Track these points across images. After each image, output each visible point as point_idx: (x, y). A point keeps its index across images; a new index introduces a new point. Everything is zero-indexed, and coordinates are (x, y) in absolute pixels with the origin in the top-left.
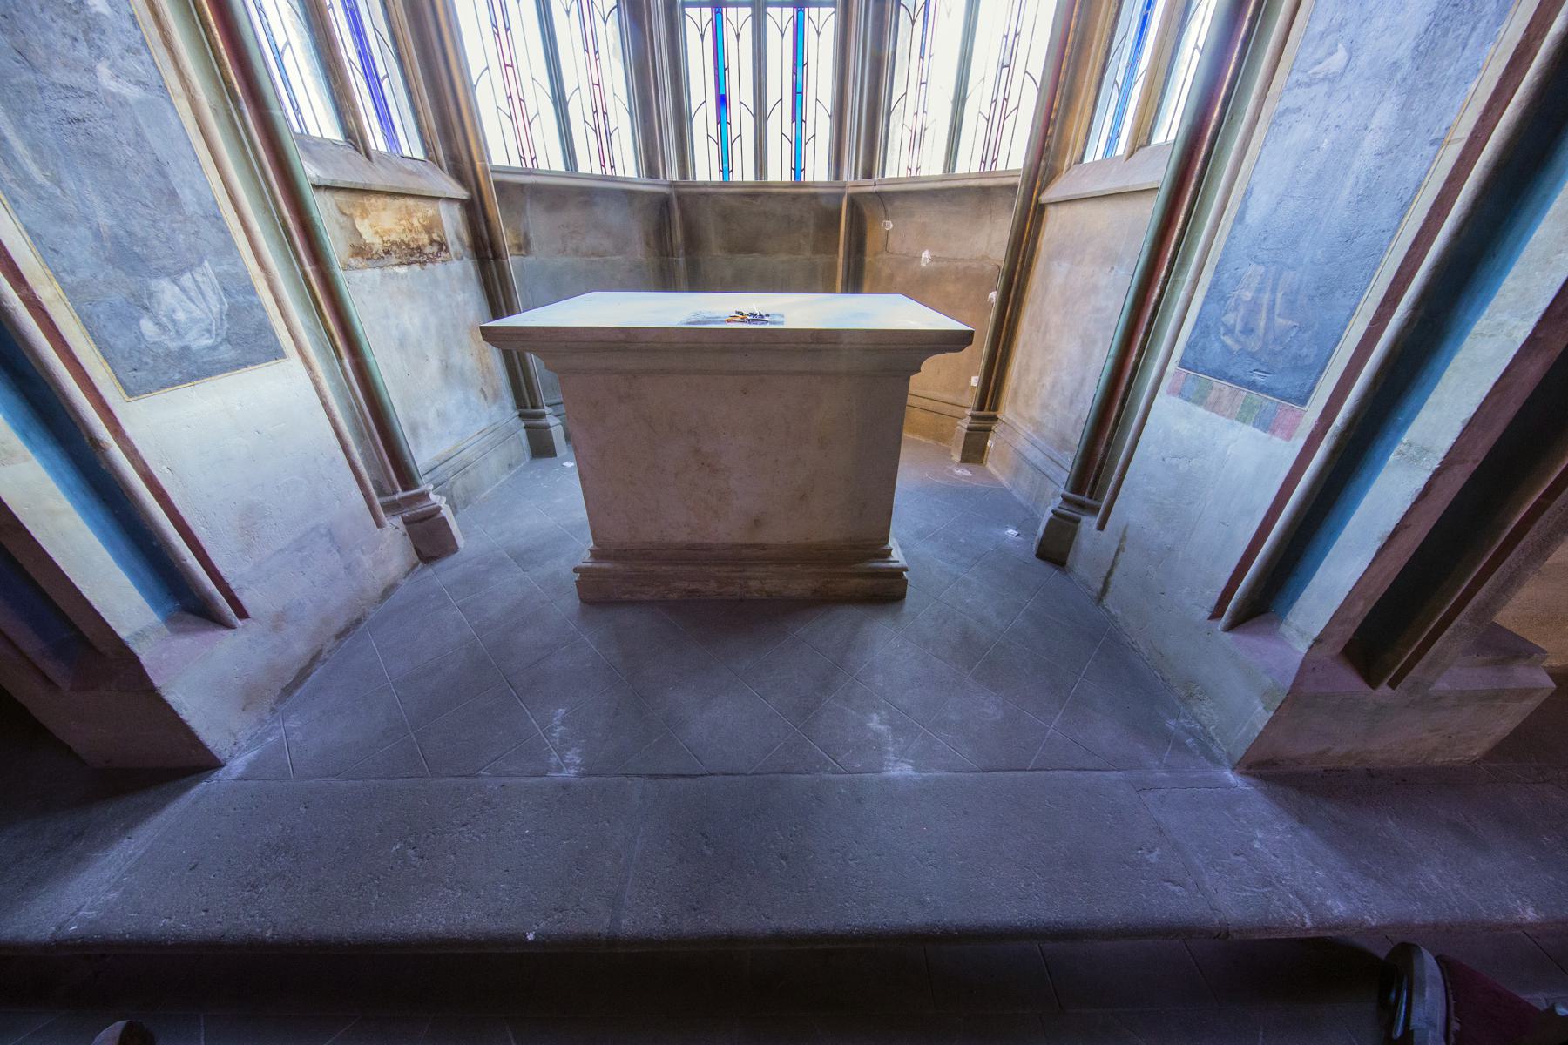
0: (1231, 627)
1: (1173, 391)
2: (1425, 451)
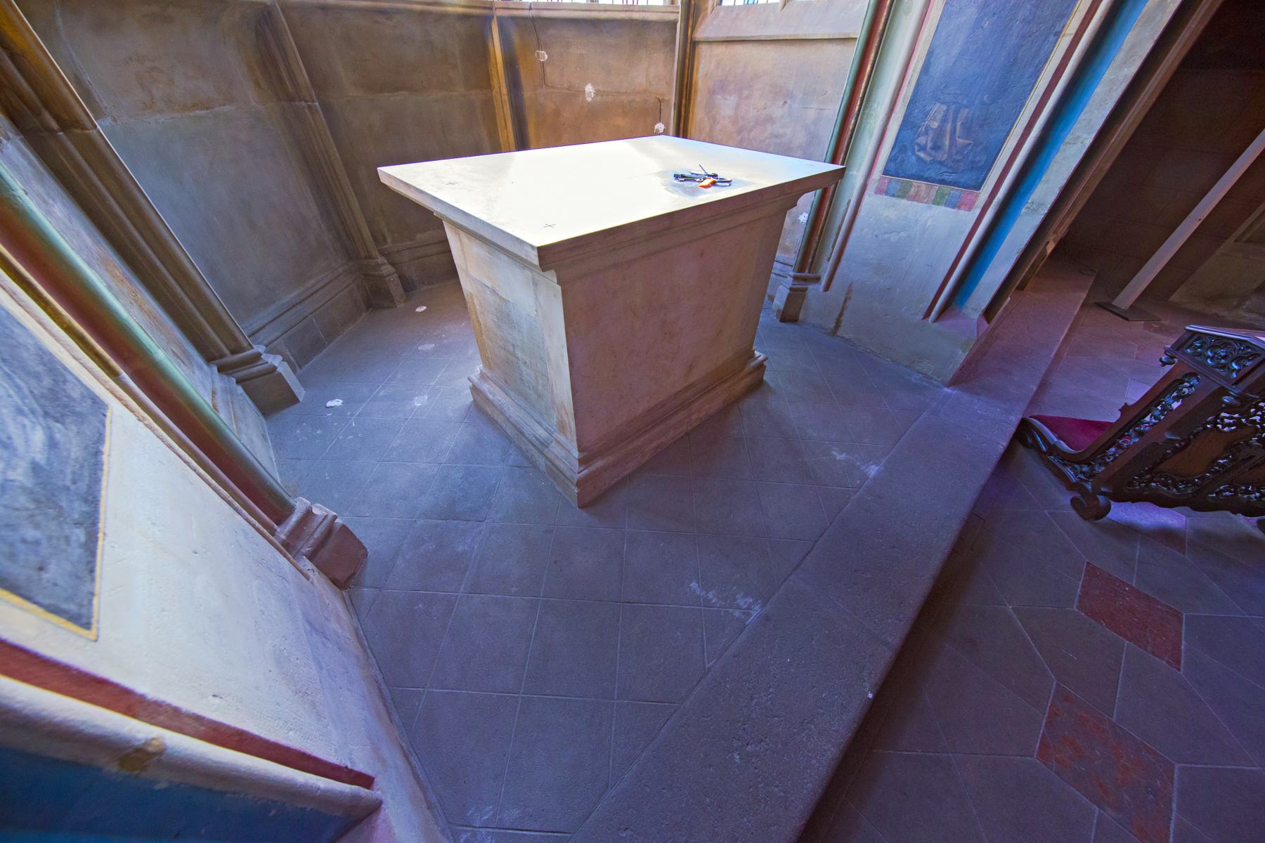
0: (937, 319)
1: (879, 191)
2: (1040, 205)
